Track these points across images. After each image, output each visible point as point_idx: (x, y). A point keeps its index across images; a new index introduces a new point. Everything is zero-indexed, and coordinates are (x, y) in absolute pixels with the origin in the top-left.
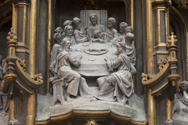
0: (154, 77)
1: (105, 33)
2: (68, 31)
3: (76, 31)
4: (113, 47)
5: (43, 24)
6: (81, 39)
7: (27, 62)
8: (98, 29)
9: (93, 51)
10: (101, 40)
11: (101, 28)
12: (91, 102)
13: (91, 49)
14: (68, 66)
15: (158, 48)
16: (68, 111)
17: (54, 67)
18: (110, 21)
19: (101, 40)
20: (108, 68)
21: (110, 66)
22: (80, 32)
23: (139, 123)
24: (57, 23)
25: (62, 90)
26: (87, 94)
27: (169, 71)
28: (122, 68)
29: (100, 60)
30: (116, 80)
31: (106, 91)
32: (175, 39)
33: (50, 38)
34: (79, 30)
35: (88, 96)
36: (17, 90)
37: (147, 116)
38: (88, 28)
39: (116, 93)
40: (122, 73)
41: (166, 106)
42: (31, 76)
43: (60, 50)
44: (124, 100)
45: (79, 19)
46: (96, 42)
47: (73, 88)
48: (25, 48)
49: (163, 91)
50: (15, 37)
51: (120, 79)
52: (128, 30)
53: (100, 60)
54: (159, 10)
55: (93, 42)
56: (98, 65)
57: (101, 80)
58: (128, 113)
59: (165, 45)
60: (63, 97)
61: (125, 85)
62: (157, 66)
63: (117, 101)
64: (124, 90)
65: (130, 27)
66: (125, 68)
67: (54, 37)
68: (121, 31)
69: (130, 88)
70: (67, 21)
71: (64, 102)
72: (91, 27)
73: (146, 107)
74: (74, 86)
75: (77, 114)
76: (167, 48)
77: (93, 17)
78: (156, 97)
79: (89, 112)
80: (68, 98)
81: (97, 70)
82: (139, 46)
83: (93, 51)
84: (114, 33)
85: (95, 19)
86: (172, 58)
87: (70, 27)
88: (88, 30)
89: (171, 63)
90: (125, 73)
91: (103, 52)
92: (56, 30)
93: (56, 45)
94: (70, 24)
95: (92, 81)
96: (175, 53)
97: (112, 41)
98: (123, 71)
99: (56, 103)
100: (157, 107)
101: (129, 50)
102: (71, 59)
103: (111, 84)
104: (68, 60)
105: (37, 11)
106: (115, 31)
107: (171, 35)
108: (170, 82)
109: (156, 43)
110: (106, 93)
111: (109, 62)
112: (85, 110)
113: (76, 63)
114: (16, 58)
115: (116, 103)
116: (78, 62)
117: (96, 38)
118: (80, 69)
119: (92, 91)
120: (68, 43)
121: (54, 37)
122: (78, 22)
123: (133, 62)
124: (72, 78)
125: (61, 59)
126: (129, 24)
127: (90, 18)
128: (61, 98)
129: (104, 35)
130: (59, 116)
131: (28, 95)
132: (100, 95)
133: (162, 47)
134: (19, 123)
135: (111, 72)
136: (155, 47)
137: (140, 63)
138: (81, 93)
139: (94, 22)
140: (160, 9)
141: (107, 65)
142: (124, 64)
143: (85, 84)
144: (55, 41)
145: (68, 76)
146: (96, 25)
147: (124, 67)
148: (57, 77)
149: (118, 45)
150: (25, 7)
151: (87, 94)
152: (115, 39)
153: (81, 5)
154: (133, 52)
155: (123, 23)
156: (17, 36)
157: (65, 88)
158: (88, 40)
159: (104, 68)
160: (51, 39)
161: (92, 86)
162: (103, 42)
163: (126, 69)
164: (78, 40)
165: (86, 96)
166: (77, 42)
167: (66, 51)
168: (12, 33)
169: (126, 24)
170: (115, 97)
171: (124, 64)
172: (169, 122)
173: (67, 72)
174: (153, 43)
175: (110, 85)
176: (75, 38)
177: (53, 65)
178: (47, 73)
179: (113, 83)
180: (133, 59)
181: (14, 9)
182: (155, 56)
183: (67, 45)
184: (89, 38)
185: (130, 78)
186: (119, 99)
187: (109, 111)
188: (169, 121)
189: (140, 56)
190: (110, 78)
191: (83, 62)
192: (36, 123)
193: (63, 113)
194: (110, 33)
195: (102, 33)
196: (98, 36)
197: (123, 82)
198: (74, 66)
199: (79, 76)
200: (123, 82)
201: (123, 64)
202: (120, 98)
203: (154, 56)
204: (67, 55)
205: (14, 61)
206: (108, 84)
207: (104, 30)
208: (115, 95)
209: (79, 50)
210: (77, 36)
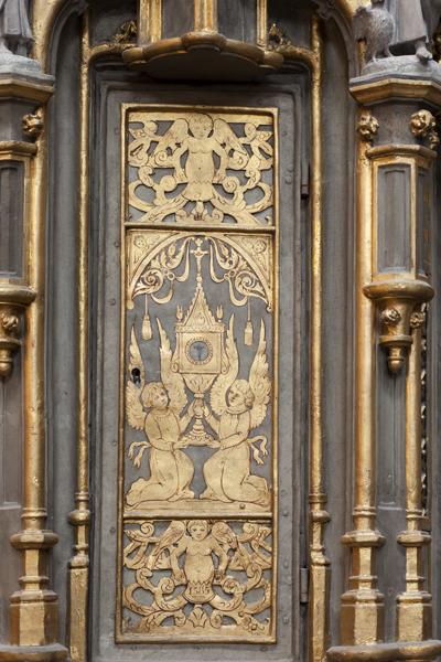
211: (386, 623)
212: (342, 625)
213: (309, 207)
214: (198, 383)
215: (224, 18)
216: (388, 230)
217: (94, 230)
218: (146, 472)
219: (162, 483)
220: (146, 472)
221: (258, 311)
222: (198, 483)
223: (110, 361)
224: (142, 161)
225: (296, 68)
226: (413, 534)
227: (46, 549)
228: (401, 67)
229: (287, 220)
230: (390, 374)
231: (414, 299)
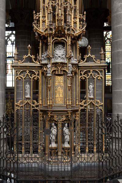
0: (68, 56)
8: (61, 48)
12: (59, 60)
24: (55, 47)
27: (70, 56)
29: (60, 54)
36: (49, 58)
42: (51, 56)
53: (60, 54)
68: (64, 48)
73: (67, 60)
95: (59, 57)
119: (59, 58)
140: (69, 46)
144: (55, 50)
178: (53, 55)
198: (57, 55)
211: (69, 103)
212: (67, 103)
213: (65, 81)
214: (59, 90)
215: (60, 72)
216: (69, 83)
217: (54, 83)
218: (56, 95)
219: (57, 96)
220: (56, 95)
221: (62, 87)
222: (59, 96)
223: (55, 89)
224: (56, 79)
225: (64, 74)
226: (70, 98)
227: (52, 99)
228: (69, 75)
229: (64, 82)
230: (69, 90)
231: (70, 87)
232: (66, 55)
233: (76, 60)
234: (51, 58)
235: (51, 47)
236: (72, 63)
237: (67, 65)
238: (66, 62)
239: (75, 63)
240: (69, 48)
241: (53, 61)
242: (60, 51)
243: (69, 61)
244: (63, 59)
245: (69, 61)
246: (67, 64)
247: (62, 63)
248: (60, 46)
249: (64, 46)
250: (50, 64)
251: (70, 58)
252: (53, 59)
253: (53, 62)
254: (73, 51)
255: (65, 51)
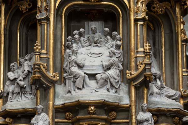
0: (135, 73)
1: (102, 40)
2: (76, 40)
3: (82, 39)
4: (107, 50)
5: (59, 33)
6: (85, 44)
7: (48, 65)
9: (93, 54)
10: (99, 45)
11: (99, 36)
12: (91, 93)
13: (92, 52)
14: (76, 67)
15: (138, 52)
16: (76, 100)
17: (67, 67)
18: (106, 31)
19: (99, 45)
20: (103, 67)
21: (104, 67)
22: (84, 39)
23: (124, 105)
24: (69, 33)
25: (72, 83)
26: (89, 86)
27: (145, 70)
28: (112, 68)
29: (97, 62)
30: (108, 77)
31: (102, 85)
32: (149, 46)
33: (63, 43)
34: (84, 37)
35: (90, 88)
36: (41, 84)
37: (131, 100)
38: (90, 36)
39: (108, 86)
40: (112, 72)
41: (143, 92)
42: (51, 74)
43: (70, 54)
44: (114, 91)
45: (84, 30)
46: (96, 46)
47: (79, 82)
48: (46, 54)
49: (140, 83)
50: (39, 47)
51: (111, 76)
52: (118, 38)
54: (139, 24)
55: (93, 46)
56: (96, 66)
57: (98, 76)
58: (117, 99)
59: (143, 50)
60: (72, 89)
61: (114, 80)
62: (137, 66)
63: (109, 91)
64: (114, 84)
65: (119, 36)
66: (115, 68)
67: (67, 44)
68: (114, 38)
69: (118, 82)
70: (76, 32)
71: (73, 93)
72: (92, 35)
73: (129, 93)
74: (80, 81)
75: (82, 102)
76: (144, 52)
77: (94, 28)
78: (136, 88)
79: (89, 101)
80: (76, 89)
81: (95, 69)
82: (125, 49)
83: (93, 54)
84: (108, 40)
85: (95, 30)
86: (147, 61)
87: (77, 36)
88: (90, 38)
89: (146, 64)
90: (115, 71)
91: (100, 55)
92: (67, 39)
93: (68, 51)
94: (77, 33)
95: (92, 76)
96: (149, 57)
97: (107, 45)
98: (113, 70)
99: (68, 93)
100: (136, 94)
101: (118, 54)
102: (79, 62)
103: (105, 80)
104: (76, 63)
105: (54, 27)
106: (109, 37)
107: (147, 44)
108: (146, 77)
109: (137, 49)
110: (101, 86)
111: (104, 64)
112: (87, 100)
113: (81, 65)
114: (40, 63)
115: (108, 93)
116: (83, 64)
117: (95, 43)
118: (84, 68)
119: (92, 83)
120: (76, 51)
121: (67, 44)
122: (83, 32)
123: (121, 62)
124: (79, 76)
125: (71, 62)
126: (119, 34)
127: (91, 29)
128: (71, 89)
129: (101, 41)
130: (70, 103)
131: (49, 88)
132: (98, 88)
133: (141, 51)
134: (43, 108)
135: (105, 71)
136: (136, 51)
137: (126, 61)
138: (85, 86)
139: (94, 32)
140: (140, 23)
141: (102, 65)
142: (114, 65)
143: (87, 79)
145: (76, 75)
146: (96, 34)
147: (114, 67)
148: (68, 74)
149: (110, 51)
150: (46, 24)
151: (89, 86)
152: (109, 43)
153: (86, 15)
154: (121, 55)
155: (115, 32)
156: (41, 47)
157: (74, 82)
158: (90, 45)
159: (101, 68)
160: (64, 44)
161: (92, 80)
162: (100, 47)
163: (115, 69)
164: (84, 45)
165: (88, 88)
166: (83, 47)
167: (75, 56)
168: (37, 45)
169: (116, 33)
170: (108, 89)
171: (114, 65)
172: (145, 106)
173: (75, 72)
174: (135, 48)
175: (104, 81)
176: (81, 43)
177: (66, 65)
178: (62, 70)
179: (106, 80)
180: (121, 59)
181: (38, 25)
182: (136, 57)
183: (75, 52)
184: (91, 44)
185: (118, 74)
186: (110, 90)
187: (103, 101)
188: (144, 104)
189: (126, 55)
190: (104, 76)
191: (86, 63)
192: (54, 106)
193: (73, 101)
194: (106, 39)
195: (100, 40)
196: (97, 42)
197: (114, 78)
198: (80, 67)
199: (83, 74)
200: (114, 78)
201: (113, 65)
202: (111, 89)
203: (135, 58)
204: (75, 59)
205: (39, 65)
206: (103, 80)
207: (101, 37)
208: (108, 88)
209: (83, 53)
210: (82, 42)
232: (126, 66)
233: (172, 92)
234: (54, 83)
235: (50, 30)
236: (153, 107)
237: (129, 117)
238: (125, 102)
239: (171, 108)
240: (138, 33)
241: (62, 96)
242: (93, 55)
243: (140, 97)
244: (111, 85)
245: (140, 97)
246: (128, 110)
247: (103, 106)
248: (94, 25)
249: (115, 28)
250: (46, 111)
251: (142, 84)
252: (60, 89)
253: (59, 102)
254: (157, 54)
255: (118, 47)
